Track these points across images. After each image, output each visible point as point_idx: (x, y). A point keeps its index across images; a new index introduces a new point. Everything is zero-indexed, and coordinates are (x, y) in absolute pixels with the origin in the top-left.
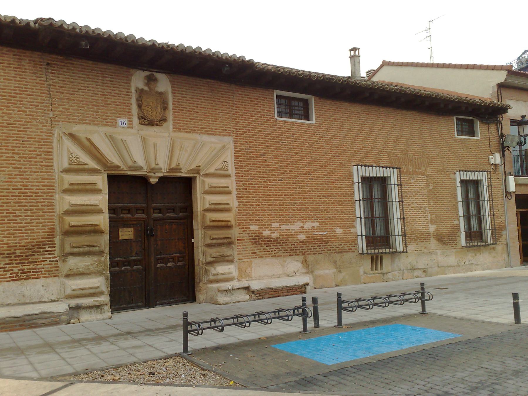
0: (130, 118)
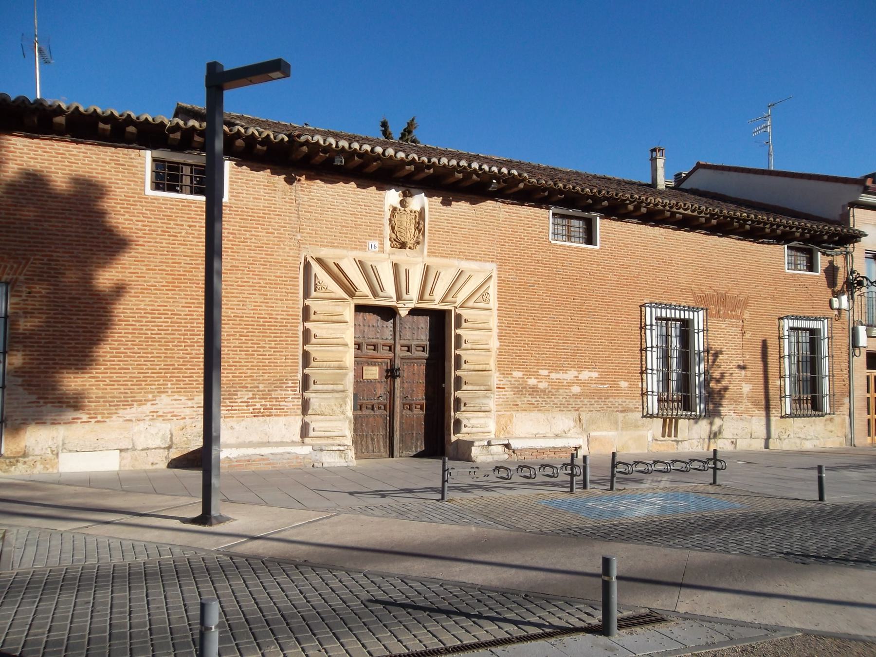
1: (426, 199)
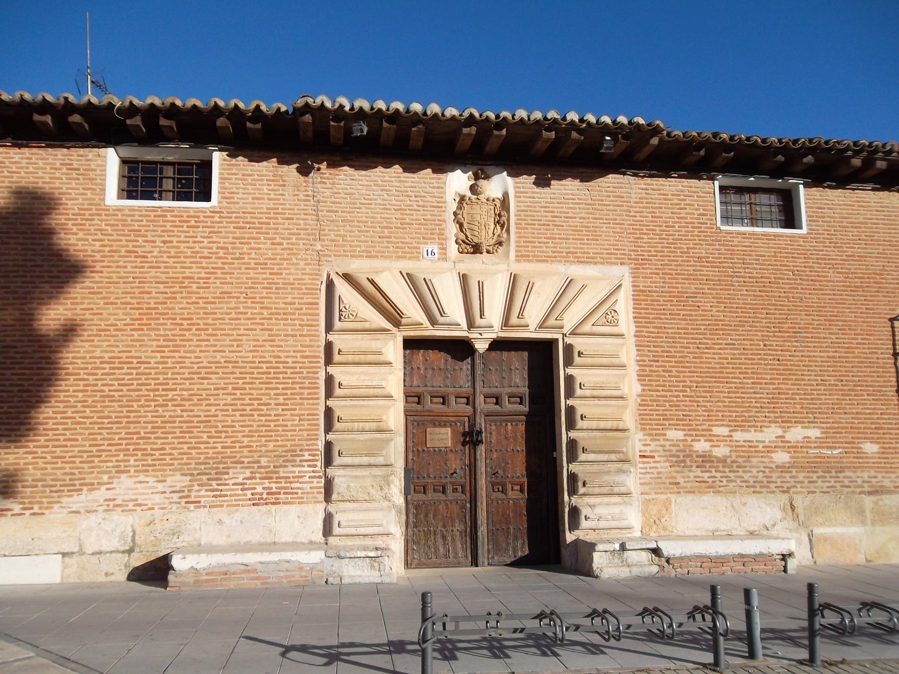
0: (442, 244)
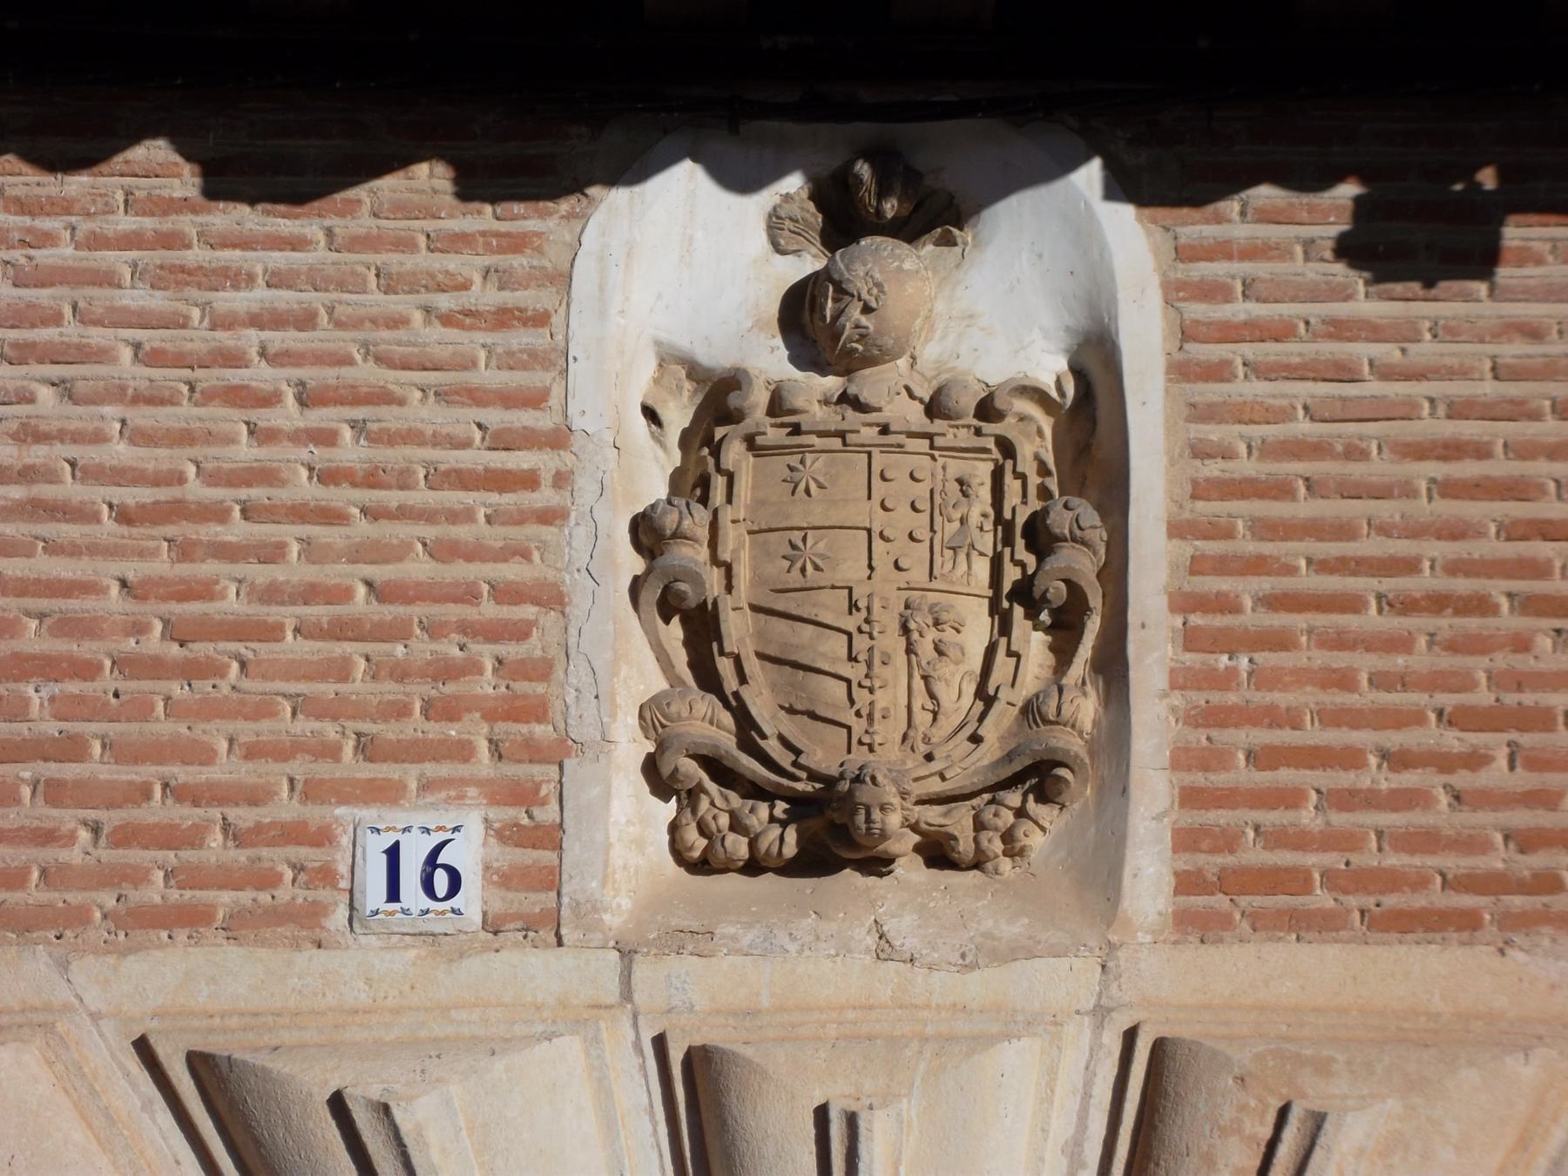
0: (525, 796)
1: (1129, 237)
